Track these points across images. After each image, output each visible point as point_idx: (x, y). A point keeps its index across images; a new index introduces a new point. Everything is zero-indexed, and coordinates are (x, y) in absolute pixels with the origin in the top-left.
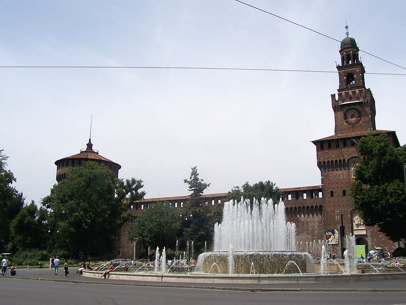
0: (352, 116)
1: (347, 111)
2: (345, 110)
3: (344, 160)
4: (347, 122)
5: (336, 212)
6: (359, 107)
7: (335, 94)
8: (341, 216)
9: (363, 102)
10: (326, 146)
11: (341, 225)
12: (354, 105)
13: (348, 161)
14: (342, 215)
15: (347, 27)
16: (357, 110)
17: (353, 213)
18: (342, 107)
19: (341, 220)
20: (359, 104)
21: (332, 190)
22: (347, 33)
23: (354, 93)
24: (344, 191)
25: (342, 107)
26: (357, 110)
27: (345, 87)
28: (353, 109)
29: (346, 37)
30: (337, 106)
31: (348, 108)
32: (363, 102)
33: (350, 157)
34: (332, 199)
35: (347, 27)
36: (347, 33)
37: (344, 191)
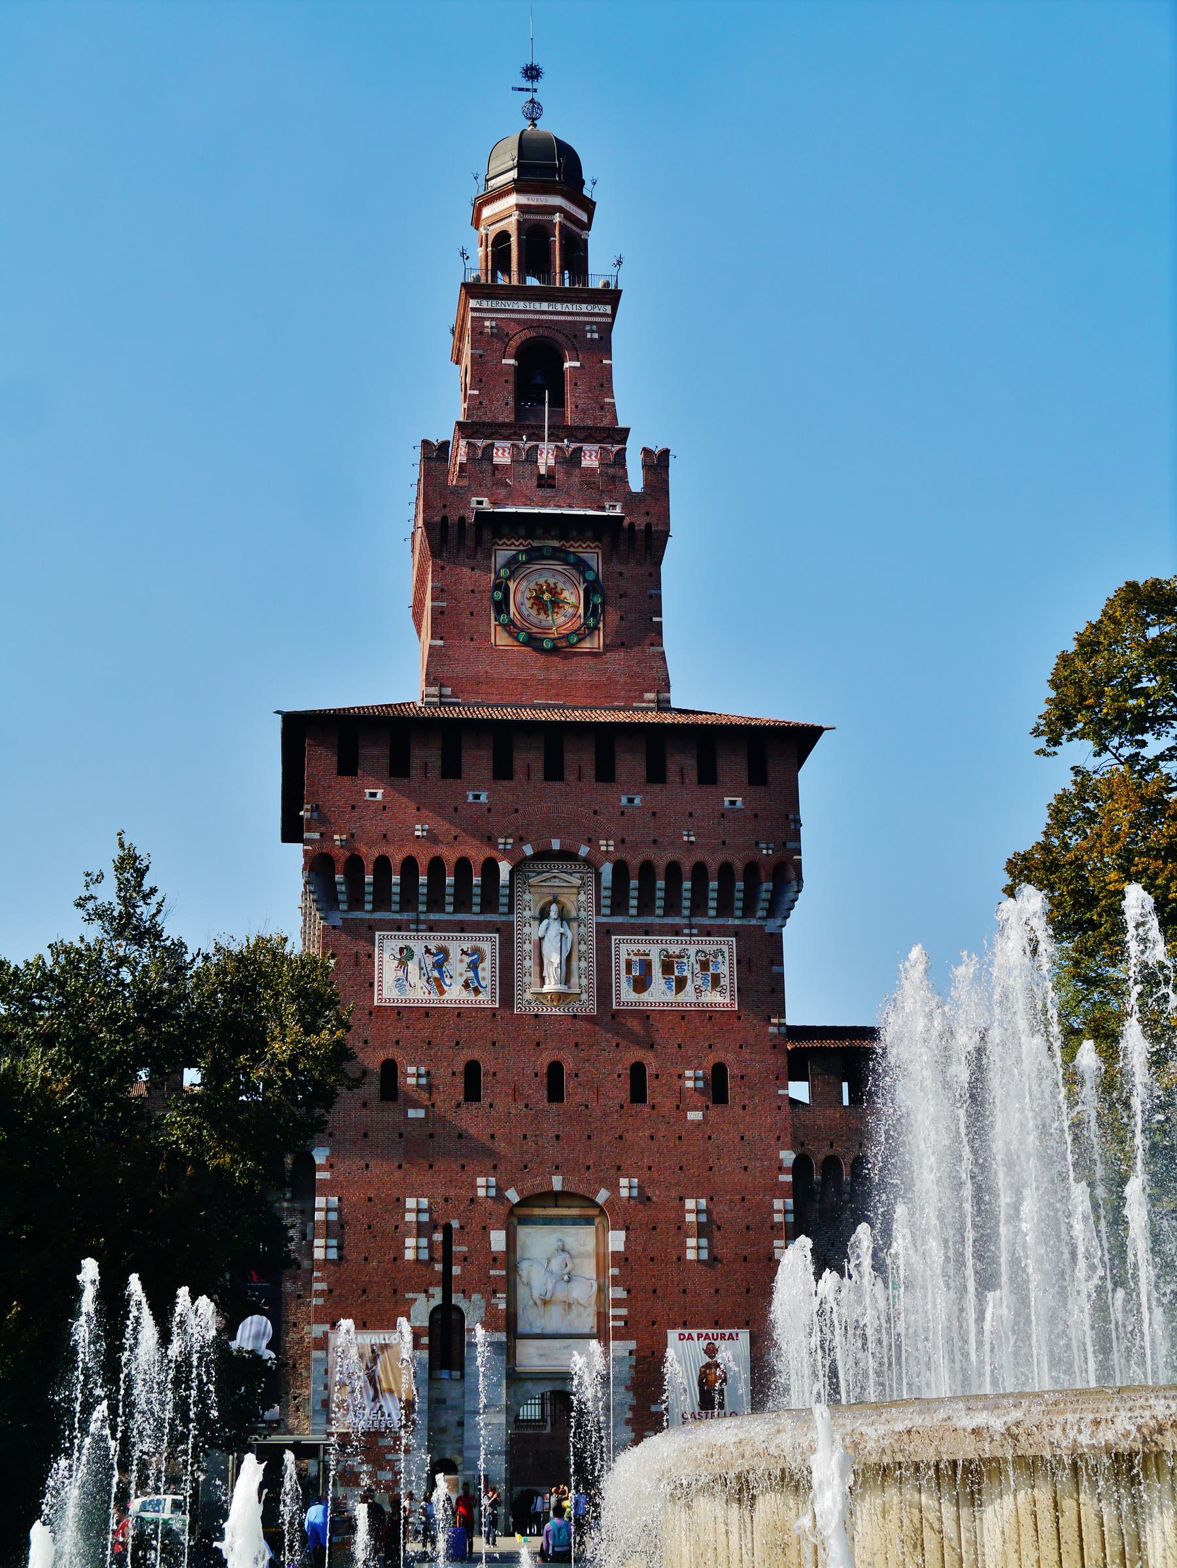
0: (547, 602)
1: (512, 563)
2: (502, 555)
3: (490, 868)
4: (510, 627)
5: (411, 1203)
6: (593, 557)
7: (445, 445)
8: (438, 1237)
9: (626, 522)
10: (375, 753)
11: (437, 1301)
12: (564, 536)
13: (511, 873)
14: (447, 1230)
15: (532, 73)
16: (581, 566)
17: (526, 1221)
18: (487, 535)
19: (438, 1267)
20: (597, 538)
21: (392, 1053)
22: (534, 112)
23: (572, 461)
24: (472, 1071)
25: (487, 535)
26: (581, 566)
27: (507, 416)
28: (559, 555)
29: (526, 125)
30: (453, 518)
31: (520, 545)
32: (626, 522)
33: (528, 850)
34: (389, 1115)
35: (532, 73)
36: (534, 112)
37: (472, 1071)
